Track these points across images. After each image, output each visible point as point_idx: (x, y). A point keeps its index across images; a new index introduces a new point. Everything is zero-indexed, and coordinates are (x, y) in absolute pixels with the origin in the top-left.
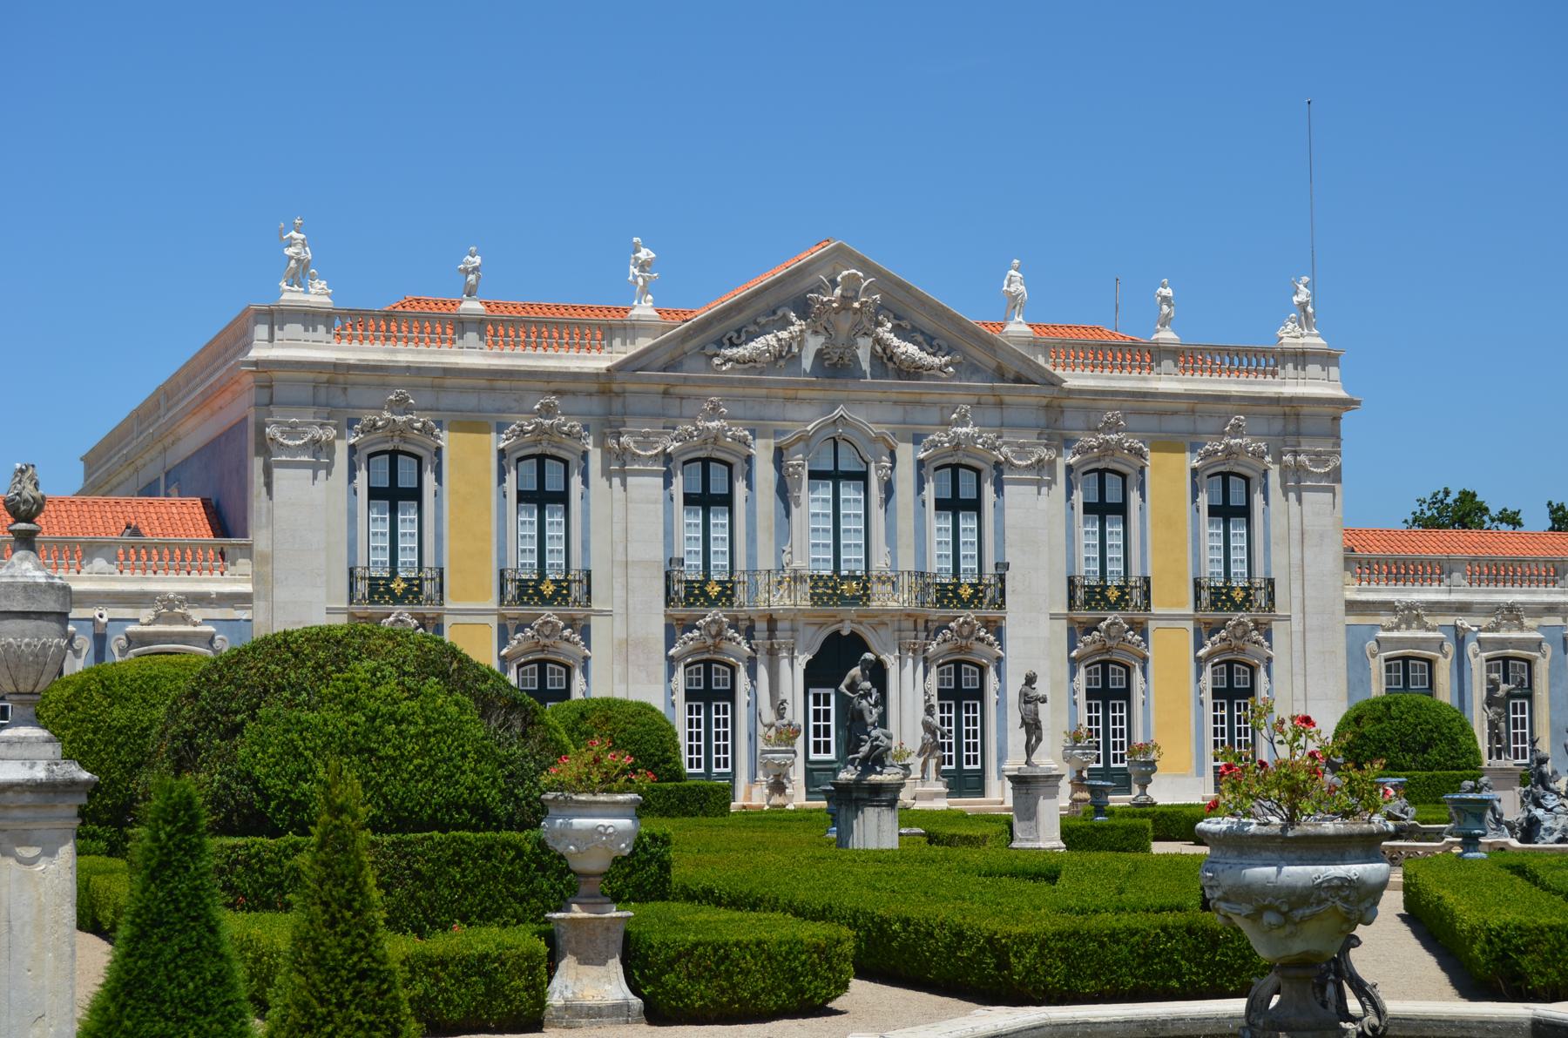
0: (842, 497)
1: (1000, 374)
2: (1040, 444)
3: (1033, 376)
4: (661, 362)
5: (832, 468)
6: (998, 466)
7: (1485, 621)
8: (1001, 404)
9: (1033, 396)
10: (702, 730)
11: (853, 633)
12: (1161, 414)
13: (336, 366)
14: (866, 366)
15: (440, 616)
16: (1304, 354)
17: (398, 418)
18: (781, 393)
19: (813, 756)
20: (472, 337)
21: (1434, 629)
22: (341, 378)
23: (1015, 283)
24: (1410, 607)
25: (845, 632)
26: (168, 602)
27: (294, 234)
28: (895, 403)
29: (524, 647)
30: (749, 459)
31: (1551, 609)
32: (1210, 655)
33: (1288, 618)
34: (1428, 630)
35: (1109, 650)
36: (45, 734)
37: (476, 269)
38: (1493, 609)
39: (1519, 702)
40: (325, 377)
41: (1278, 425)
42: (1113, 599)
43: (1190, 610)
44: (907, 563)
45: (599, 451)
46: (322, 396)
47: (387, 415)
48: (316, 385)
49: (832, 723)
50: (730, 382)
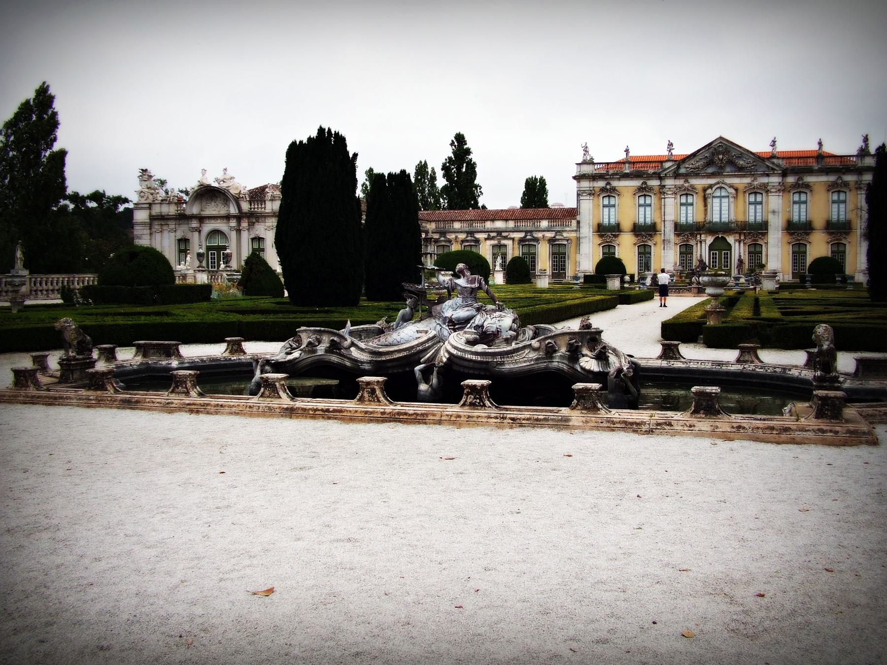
11: (722, 237)
25: (720, 236)
32: (831, 241)
35: (799, 240)
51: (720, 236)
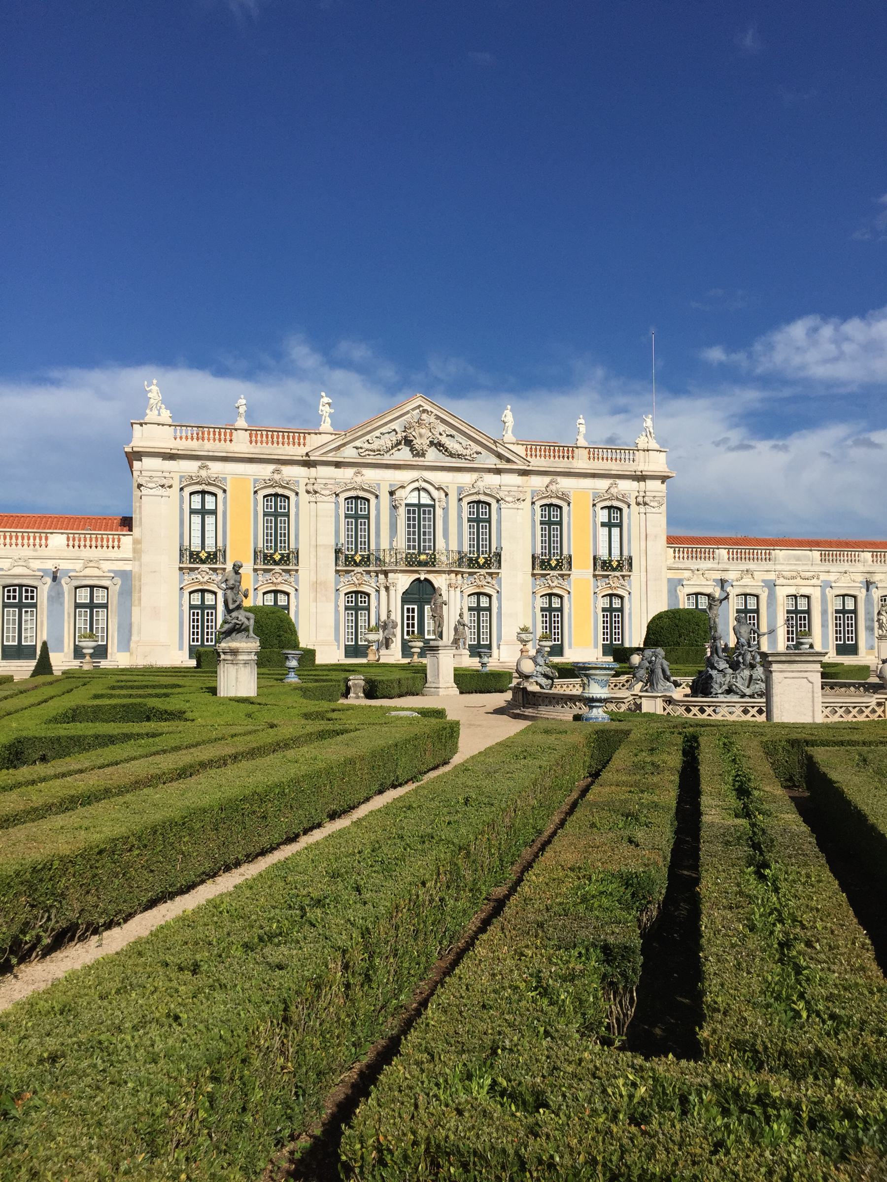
25: (422, 578)
42: (553, 565)
44: (454, 546)
51: (422, 578)
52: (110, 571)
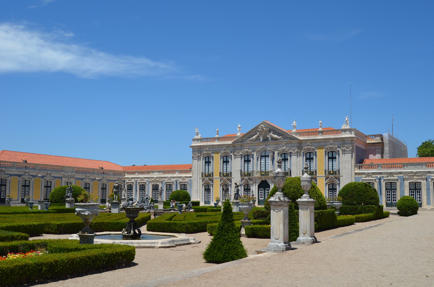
0: (266, 159)
1: (291, 139)
2: (297, 149)
3: (294, 138)
4: (240, 142)
5: (265, 155)
6: (291, 153)
7: (385, 176)
8: (291, 143)
9: (295, 142)
10: (332, 195)
11: (265, 180)
12: (319, 142)
13: (201, 146)
14: (270, 139)
15: (213, 179)
16: (346, 130)
17: (206, 152)
18: (258, 144)
19: (260, 199)
20: (217, 140)
21: (374, 177)
22: (202, 147)
23: (294, 123)
24: (369, 173)
26: (183, 178)
27: (196, 129)
28: (275, 144)
29: (223, 183)
30: (253, 155)
31: (400, 173)
32: (328, 183)
33: (343, 176)
34: (373, 177)
36: (308, 195)
37: (218, 131)
38: (386, 173)
39: (394, 191)
40: (199, 147)
41: (341, 142)
43: (324, 175)
45: (233, 155)
46: (199, 150)
47: (205, 152)
48: (198, 148)
49: (263, 194)
50: (248, 144)
51: (264, 180)
52: (187, 180)
